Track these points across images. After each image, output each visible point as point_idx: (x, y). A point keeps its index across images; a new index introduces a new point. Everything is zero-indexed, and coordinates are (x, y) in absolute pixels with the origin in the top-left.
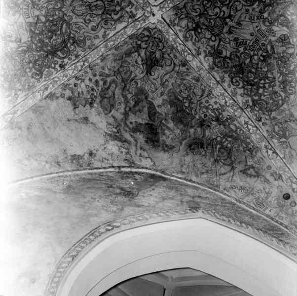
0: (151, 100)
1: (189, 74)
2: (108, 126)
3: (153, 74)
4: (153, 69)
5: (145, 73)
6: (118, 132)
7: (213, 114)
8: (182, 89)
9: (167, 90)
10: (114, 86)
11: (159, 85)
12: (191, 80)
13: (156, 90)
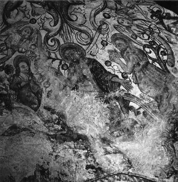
0: (91, 57)
2: (46, 125)
3: (74, 18)
4: (69, 11)
5: (59, 23)
6: (63, 128)
9: (110, 36)
10: (26, 65)
11: (94, 32)
13: (92, 40)
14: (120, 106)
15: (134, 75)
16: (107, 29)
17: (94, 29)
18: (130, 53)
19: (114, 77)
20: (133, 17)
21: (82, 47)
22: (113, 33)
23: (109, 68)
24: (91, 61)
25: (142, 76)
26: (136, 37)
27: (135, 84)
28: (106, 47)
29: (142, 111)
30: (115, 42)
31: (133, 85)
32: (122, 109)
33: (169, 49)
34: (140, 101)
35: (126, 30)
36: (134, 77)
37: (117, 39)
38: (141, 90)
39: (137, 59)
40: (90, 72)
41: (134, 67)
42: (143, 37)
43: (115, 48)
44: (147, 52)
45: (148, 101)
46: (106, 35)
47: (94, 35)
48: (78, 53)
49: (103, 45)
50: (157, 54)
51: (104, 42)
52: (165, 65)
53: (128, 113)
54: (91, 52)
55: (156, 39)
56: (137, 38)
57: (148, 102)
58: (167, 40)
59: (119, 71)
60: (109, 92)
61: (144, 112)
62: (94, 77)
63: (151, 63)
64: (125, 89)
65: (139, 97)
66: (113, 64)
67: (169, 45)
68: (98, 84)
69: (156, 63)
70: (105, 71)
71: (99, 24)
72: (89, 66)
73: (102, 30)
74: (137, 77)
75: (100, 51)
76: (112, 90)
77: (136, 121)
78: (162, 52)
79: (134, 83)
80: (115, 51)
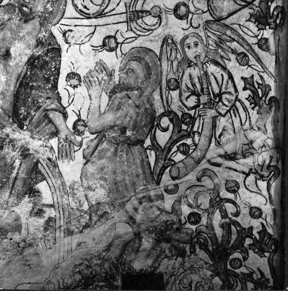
1: (252, 61)
7: (219, 232)
8: (186, 79)
9: (137, 43)
11: (122, 8)
12: (240, 85)
13: (100, 15)
14: (17, 173)
15: (97, 140)
16: (148, 30)
17: (128, 5)
18: (130, 101)
19: (60, 112)
20: (222, 57)
21: (65, 6)
22: (148, 45)
23: (65, 89)
24: (50, 44)
25: (109, 154)
26: (178, 87)
27: (84, 157)
28: (105, 51)
29: (50, 213)
30: (129, 61)
31: (79, 155)
32: (17, 181)
33: (200, 150)
34: (63, 194)
35: (175, 64)
36: (93, 144)
37: (139, 60)
38: (84, 175)
39: (129, 122)
40: (25, 59)
41: (112, 127)
42: (188, 97)
43: (117, 69)
44: (159, 125)
45: (78, 204)
46: (134, 35)
47: (114, 12)
48: (49, 5)
49: (104, 45)
50: (172, 142)
51: (113, 40)
52: (164, 168)
53: (20, 197)
54: (71, 31)
55: (203, 119)
56: (174, 90)
57: (75, 207)
58: (218, 134)
59: (79, 112)
60: (22, 128)
61: (50, 219)
62: (23, 75)
63: (146, 147)
64: (57, 152)
65: (68, 184)
66: (82, 90)
67: (210, 142)
68: (17, 96)
69: (153, 153)
70: (55, 86)
71: (147, 7)
72: (37, 46)
73: (139, 21)
74: (99, 148)
75: (86, 47)
76: (31, 131)
77: (21, 224)
78: (184, 144)
79: (83, 154)
80: (111, 75)
